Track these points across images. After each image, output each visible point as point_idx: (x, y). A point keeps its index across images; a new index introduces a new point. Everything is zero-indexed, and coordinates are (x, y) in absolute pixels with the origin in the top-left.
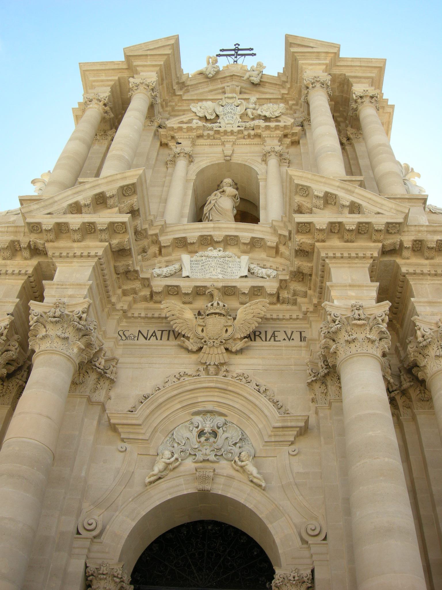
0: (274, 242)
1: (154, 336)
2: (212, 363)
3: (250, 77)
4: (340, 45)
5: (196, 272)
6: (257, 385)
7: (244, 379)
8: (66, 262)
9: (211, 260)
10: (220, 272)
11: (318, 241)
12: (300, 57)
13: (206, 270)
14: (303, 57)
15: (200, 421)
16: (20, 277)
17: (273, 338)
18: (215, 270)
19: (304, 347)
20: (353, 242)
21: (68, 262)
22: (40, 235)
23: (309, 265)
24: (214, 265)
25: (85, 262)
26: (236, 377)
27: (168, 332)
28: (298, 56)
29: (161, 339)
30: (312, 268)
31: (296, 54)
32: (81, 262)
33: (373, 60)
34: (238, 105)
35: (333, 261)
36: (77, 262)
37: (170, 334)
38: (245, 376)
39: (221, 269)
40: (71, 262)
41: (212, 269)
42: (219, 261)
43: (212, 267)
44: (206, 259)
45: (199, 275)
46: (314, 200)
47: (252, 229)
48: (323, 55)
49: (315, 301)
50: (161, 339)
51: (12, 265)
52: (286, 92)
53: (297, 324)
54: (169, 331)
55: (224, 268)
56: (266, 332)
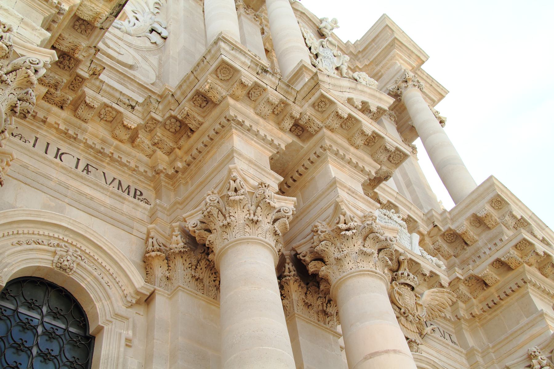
3: (324, 27)
4: (427, 58)
8: (339, 163)
9: (393, 223)
11: (527, 263)
12: (398, 46)
14: (400, 48)
16: (268, 147)
19: (464, 354)
20: (547, 277)
21: (341, 164)
22: (318, 115)
23: (498, 278)
25: (356, 174)
28: (397, 44)
30: (497, 281)
31: (396, 41)
32: (352, 171)
33: (441, 86)
34: (335, 55)
35: (532, 287)
36: (349, 170)
40: (344, 166)
44: (389, 220)
46: (507, 218)
47: (408, 207)
48: (414, 56)
49: (476, 311)
51: (265, 127)
52: (361, 67)
53: (446, 325)
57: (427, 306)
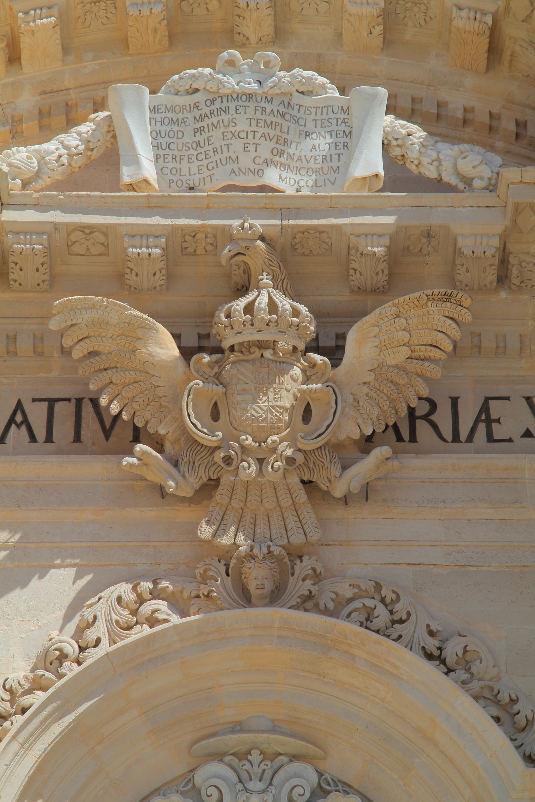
0: (484, 14)
1: (18, 426)
2: (260, 551)
5: (174, 158)
6: (432, 634)
7: (381, 610)
9: (232, 105)
10: (269, 156)
13: (215, 151)
15: (225, 779)
17: (482, 427)
18: (252, 148)
24: (246, 128)
26: (350, 600)
27: (71, 407)
29: (49, 439)
37: (84, 414)
38: (384, 593)
39: (273, 144)
41: (237, 145)
42: (264, 110)
43: (236, 136)
44: (213, 102)
45: (185, 171)
50: (49, 439)
54: (79, 401)
55: (286, 141)
56: (455, 401)
57: (370, 377)
